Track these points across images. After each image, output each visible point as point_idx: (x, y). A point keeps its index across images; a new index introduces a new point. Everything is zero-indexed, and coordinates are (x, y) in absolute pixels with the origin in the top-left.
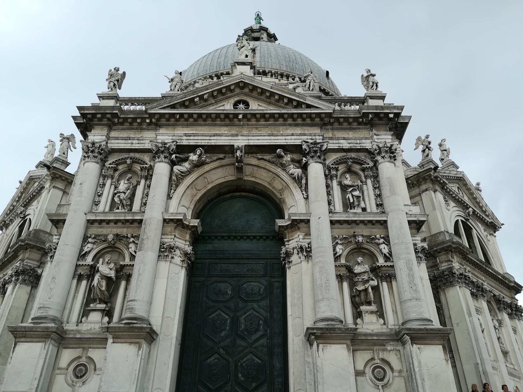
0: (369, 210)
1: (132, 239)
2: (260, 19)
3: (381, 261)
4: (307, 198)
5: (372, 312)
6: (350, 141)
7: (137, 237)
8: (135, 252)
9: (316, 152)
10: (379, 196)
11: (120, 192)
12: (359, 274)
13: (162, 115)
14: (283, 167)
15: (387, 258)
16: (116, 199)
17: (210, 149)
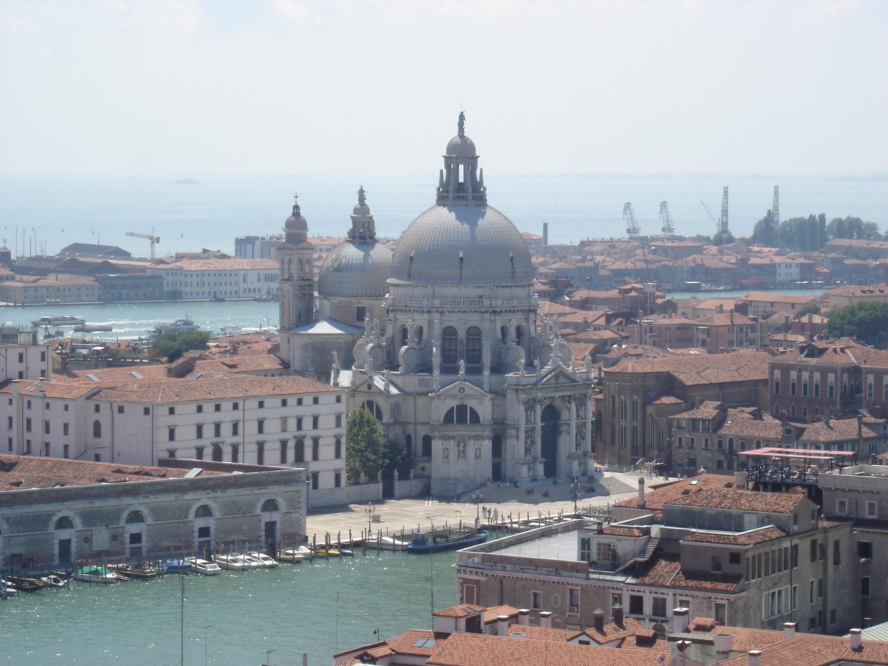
4: (569, 414)
10: (585, 412)
14: (565, 402)
15: (584, 433)
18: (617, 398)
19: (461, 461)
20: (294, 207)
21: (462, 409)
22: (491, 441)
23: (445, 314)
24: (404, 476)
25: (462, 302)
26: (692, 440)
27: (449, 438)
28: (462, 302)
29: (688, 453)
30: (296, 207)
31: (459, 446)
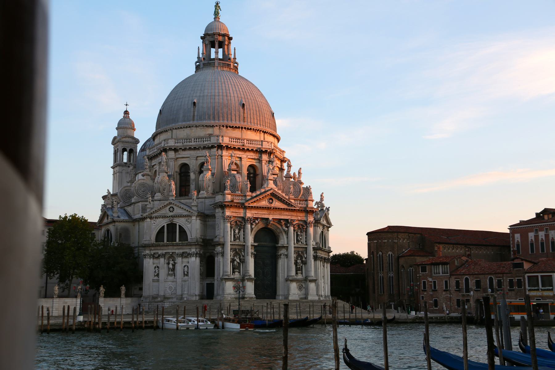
0: (303, 242)
1: (243, 251)
2: (219, 7)
3: (304, 259)
4: (287, 238)
5: (300, 273)
6: (301, 217)
7: (244, 250)
8: (244, 255)
9: (292, 223)
10: (306, 238)
11: (237, 234)
12: (299, 263)
13: (249, 206)
14: (281, 226)
15: (306, 258)
16: (236, 237)
17: (262, 219)
18: (375, 253)
19: (171, 278)
20: (124, 112)
21: (172, 227)
22: (198, 260)
23: (179, 152)
24: (112, 293)
25: (193, 139)
26: (435, 282)
27: (159, 257)
28: (193, 139)
29: (431, 295)
30: (126, 113)
31: (168, 264)
